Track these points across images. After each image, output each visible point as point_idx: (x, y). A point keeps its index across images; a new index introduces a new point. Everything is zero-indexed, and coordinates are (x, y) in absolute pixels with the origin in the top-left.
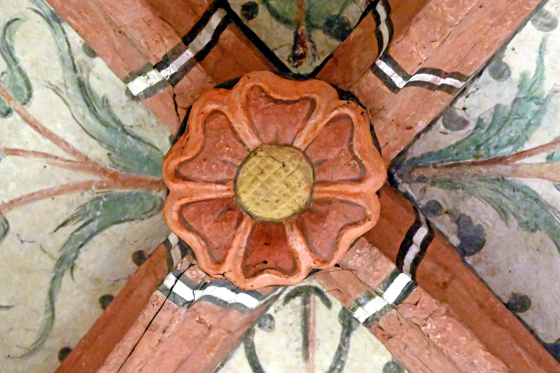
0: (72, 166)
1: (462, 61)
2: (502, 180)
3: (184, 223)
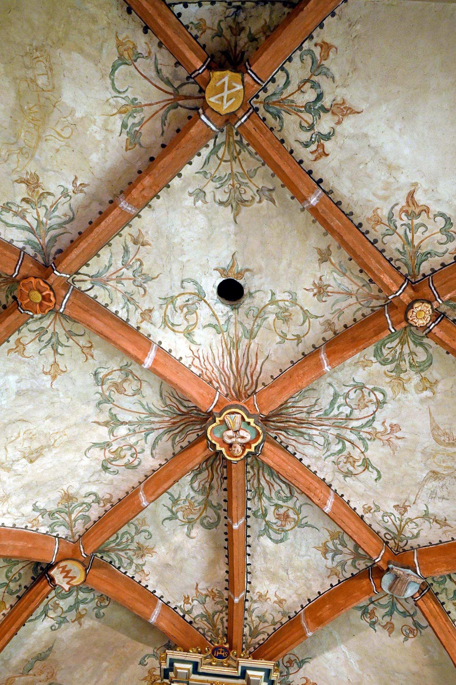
0: (56, 320)
1: (14, 260)
2: (46, 247)
3: (44, 312)
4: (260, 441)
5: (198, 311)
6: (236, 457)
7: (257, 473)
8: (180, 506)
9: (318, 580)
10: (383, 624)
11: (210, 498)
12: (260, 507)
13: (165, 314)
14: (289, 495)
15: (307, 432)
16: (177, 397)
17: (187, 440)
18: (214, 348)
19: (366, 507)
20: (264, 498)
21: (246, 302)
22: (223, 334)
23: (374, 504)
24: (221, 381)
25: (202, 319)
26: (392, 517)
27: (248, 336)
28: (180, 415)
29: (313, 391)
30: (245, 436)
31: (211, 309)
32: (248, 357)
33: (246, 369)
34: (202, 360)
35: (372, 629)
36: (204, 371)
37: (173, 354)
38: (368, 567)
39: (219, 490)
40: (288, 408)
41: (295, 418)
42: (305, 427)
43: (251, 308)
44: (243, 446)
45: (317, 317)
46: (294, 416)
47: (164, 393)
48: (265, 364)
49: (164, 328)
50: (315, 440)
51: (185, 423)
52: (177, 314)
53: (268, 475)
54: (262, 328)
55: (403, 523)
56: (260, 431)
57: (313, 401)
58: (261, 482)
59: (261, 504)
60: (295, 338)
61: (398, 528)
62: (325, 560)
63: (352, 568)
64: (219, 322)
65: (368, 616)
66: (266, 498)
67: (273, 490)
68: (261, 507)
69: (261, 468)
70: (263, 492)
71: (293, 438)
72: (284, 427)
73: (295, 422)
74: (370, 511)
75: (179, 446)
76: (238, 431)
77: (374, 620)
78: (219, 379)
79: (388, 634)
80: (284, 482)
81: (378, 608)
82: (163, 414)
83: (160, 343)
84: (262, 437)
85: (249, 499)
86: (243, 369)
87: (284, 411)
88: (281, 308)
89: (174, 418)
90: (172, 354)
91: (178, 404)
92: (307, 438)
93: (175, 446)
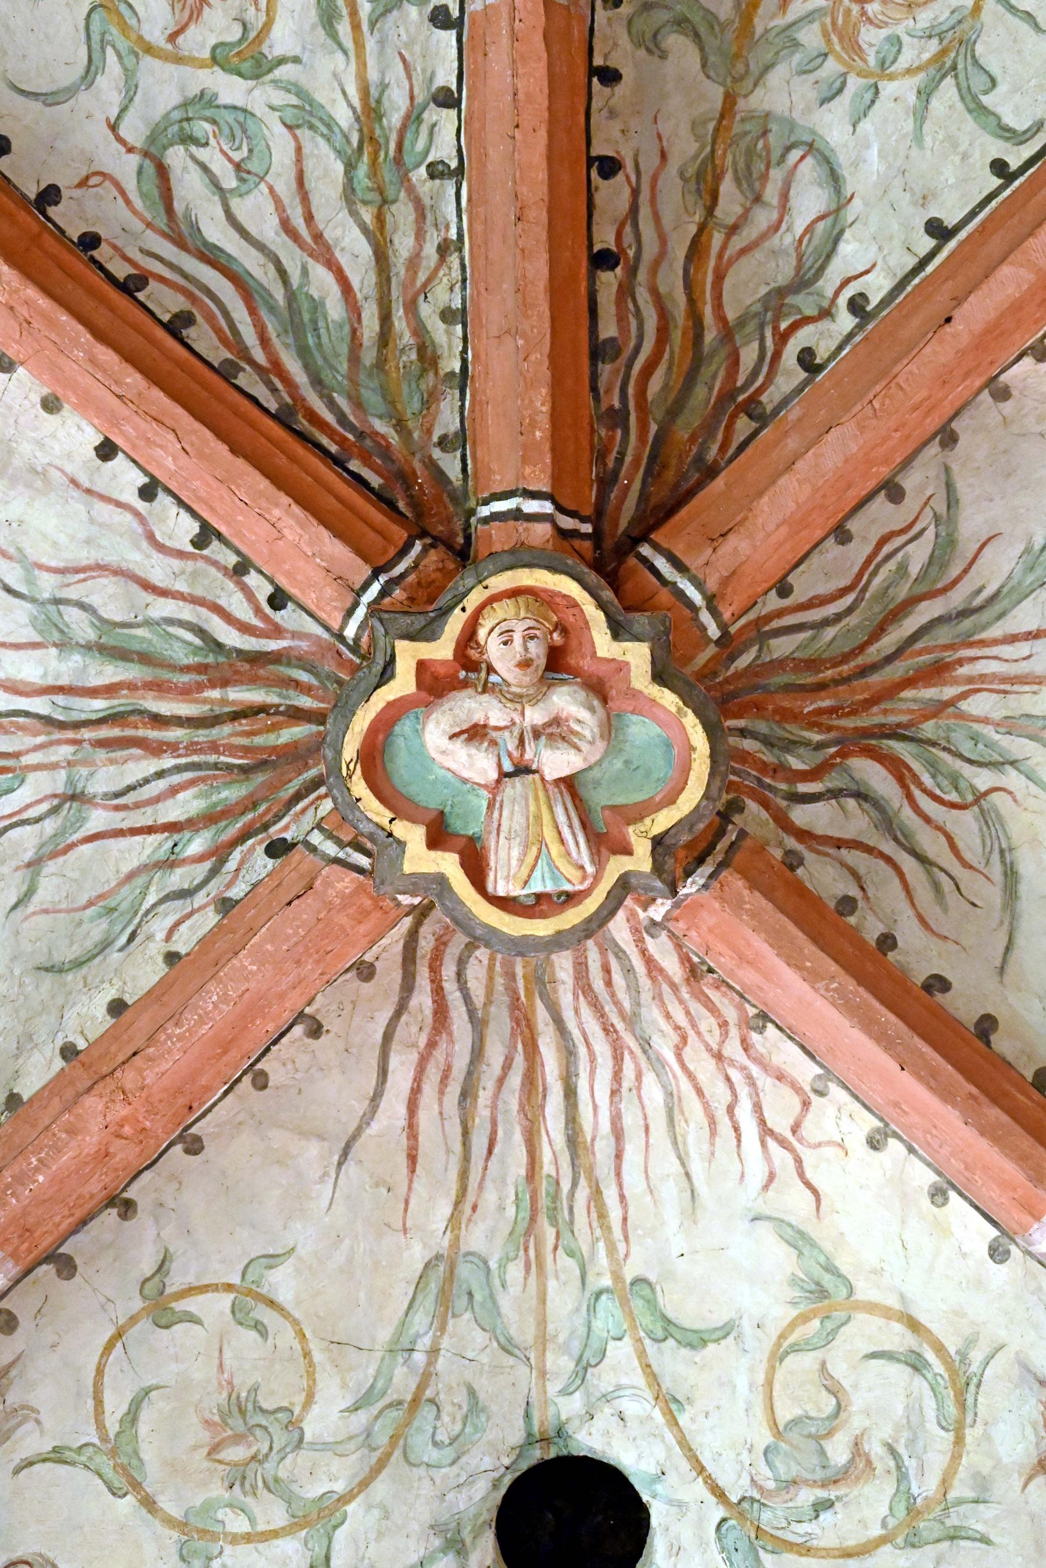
4: (363, 719)
5: (764, 1437)
6: (515, 593)
7: (399, 314)
8: (925, 17)
11: (716, 94)
12: (371, 44)
13: (959, 1440)
14: (176, 157)
15: (77, 659)
16: (908, 864)
17: (858, 551)
18: (671, 1191)
20: (343, 117)
21: (481, 1487)
22: (617, 1277)
24: (629, 971)
25: (742, 1382)
27: (464, 1270)
28: (894, 733)
29: (57, 958)
30: (458, 745)
31: (684, 1443)
32: (466, 1133)
33: (477, 1053)
34: (745, 1113)
36: (733, 1049)
37: (924, 1177)
39: (649, 163)
40: (210, 819)
41: (157, 749)
42: (93, 692)
43: (449, 1453)
44: (472, 666)
45: (57, 1456)
46: (168, 762)
47: (992, 895)
48: (361, 1107)
49: (971, 1342)
50: (23, 610)
51: (864, 671)
52: (884, 1432)
53: (317, 306)
54: (385, 1335)
56: (359, 787)
57: (47, 891)
58: (365, 250)
59: (362, 65)
60: (180, 1306)
64: (642, 1354)
66: (330, 123)
67: (285, 188)
68: (359, 46)
69: (369, 357)
70: (350, 167)
71: (163, 608)
72: (225, 683)
73: (158, 720)
75: (911, 504)
76: (504, 775)
78: (645, 982)
80: (211, 256)
82: (1004, 741)
83: (997, 1253)
84: (350, 752)
85: (447, 99)
86: (495, 1054)
87: (231, 794)
88: (274, 1486)
89: (940, 708)
90: (933, 1177)
91: (907, 813)
92: (72, 614)
93: (942, 508)
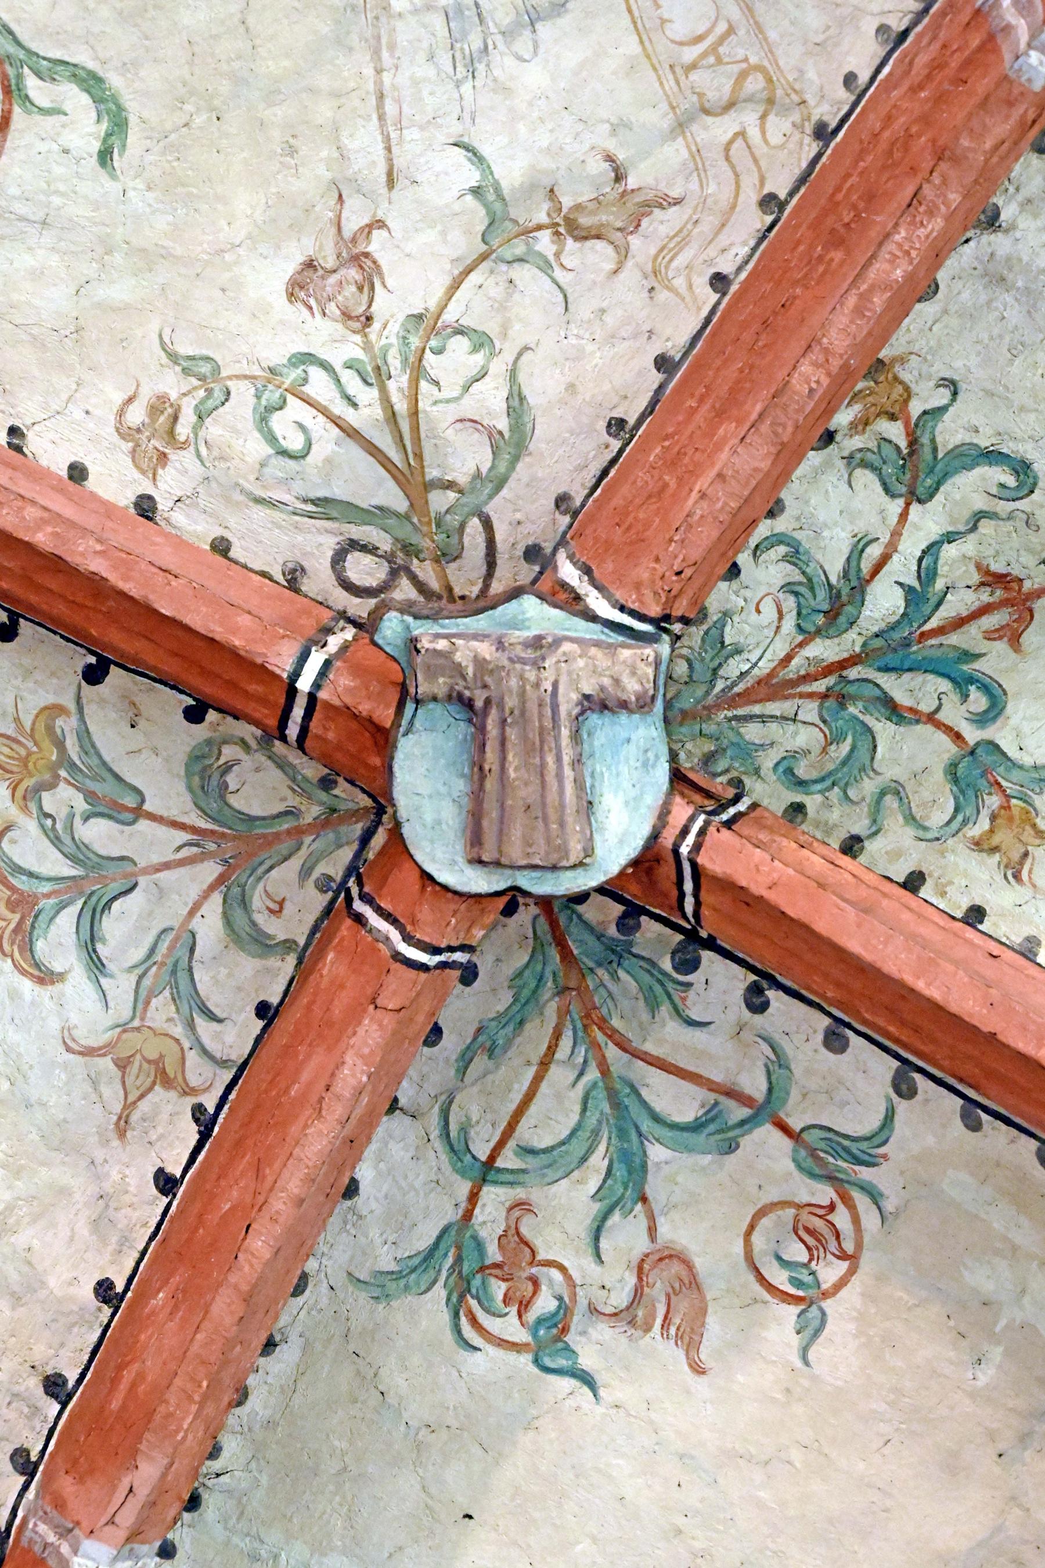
9: (64, 1192)
10: (620, 1298)
19: (136, 415)
23: (174, 357)
26: (319, 385)
35: (567, 1383)
38: (343, 886)
55: (398, 385)
61: (385, 442)
62: (45, 993)
63: (248, 965)
65: (498, 1289)
74: (171, 433)
77: (545, 1304)
79: (674, 1355)
81: (535, 1195)
